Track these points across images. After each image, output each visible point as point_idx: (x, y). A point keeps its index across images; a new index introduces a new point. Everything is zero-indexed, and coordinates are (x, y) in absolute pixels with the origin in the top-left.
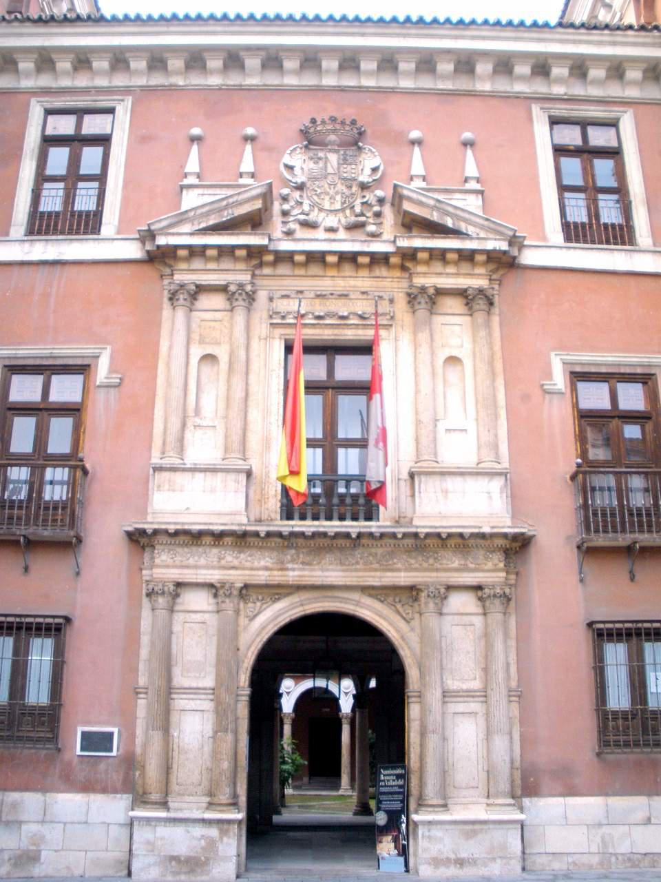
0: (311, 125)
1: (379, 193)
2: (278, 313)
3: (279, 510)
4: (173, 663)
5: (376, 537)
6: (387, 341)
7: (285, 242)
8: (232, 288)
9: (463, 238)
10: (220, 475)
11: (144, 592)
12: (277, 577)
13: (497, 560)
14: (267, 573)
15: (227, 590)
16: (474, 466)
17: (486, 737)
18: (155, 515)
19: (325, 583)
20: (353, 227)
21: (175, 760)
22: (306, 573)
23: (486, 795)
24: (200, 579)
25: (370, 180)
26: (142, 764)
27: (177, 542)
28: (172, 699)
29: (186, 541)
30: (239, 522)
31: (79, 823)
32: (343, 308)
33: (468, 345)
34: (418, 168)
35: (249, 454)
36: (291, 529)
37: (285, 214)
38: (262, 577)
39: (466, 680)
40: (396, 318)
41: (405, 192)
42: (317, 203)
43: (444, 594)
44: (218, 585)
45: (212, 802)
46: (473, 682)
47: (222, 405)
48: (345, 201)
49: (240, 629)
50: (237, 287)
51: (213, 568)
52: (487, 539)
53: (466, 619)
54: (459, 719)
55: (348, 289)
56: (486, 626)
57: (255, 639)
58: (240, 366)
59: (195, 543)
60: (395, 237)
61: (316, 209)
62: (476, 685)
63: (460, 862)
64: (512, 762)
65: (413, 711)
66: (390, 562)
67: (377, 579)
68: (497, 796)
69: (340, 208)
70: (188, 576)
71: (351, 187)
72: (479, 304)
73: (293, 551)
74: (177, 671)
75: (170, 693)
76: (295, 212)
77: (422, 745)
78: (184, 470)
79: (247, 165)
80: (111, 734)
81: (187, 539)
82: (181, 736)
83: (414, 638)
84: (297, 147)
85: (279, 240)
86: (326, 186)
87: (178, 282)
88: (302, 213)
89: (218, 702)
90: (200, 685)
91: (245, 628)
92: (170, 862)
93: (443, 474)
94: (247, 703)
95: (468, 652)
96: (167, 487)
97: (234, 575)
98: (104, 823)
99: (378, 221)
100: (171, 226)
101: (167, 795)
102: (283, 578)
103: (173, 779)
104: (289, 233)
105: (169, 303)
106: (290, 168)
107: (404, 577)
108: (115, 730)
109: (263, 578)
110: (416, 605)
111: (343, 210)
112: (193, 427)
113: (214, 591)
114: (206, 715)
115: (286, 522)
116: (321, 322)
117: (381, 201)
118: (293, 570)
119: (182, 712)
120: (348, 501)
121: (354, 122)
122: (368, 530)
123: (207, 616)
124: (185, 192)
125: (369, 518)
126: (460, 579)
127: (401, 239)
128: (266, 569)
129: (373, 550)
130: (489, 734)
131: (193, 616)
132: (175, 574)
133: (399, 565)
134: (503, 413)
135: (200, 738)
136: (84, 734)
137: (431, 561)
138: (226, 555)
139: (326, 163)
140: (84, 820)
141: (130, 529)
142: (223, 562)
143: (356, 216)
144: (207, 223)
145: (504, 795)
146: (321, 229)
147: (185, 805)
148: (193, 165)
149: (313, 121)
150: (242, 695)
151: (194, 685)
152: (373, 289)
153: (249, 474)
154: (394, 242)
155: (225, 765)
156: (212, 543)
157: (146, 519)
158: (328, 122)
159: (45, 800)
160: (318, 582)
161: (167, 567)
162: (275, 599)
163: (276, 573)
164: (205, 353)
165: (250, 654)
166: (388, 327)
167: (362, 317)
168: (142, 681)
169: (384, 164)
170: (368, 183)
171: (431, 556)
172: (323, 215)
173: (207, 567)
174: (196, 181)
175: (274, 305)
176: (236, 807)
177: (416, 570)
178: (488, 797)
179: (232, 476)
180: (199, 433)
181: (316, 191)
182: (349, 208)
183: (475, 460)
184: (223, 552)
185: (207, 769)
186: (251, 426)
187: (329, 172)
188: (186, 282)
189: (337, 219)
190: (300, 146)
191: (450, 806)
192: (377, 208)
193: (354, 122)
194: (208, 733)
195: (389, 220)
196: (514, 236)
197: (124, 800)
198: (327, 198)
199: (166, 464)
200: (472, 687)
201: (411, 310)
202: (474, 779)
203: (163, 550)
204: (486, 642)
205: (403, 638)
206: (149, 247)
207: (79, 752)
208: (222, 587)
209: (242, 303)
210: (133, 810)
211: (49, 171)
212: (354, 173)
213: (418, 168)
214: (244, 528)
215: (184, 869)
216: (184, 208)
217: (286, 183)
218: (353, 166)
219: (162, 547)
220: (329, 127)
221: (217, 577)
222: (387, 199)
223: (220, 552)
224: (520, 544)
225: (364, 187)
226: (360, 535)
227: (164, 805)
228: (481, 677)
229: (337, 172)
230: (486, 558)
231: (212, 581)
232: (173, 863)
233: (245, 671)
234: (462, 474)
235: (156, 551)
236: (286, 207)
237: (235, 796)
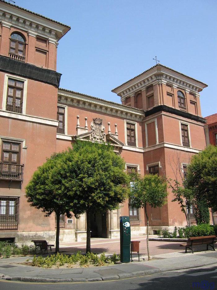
1: (105, 134)
88: (94, 135)
108: (72, 219)
117: (104, 135)
225: (102, 132)
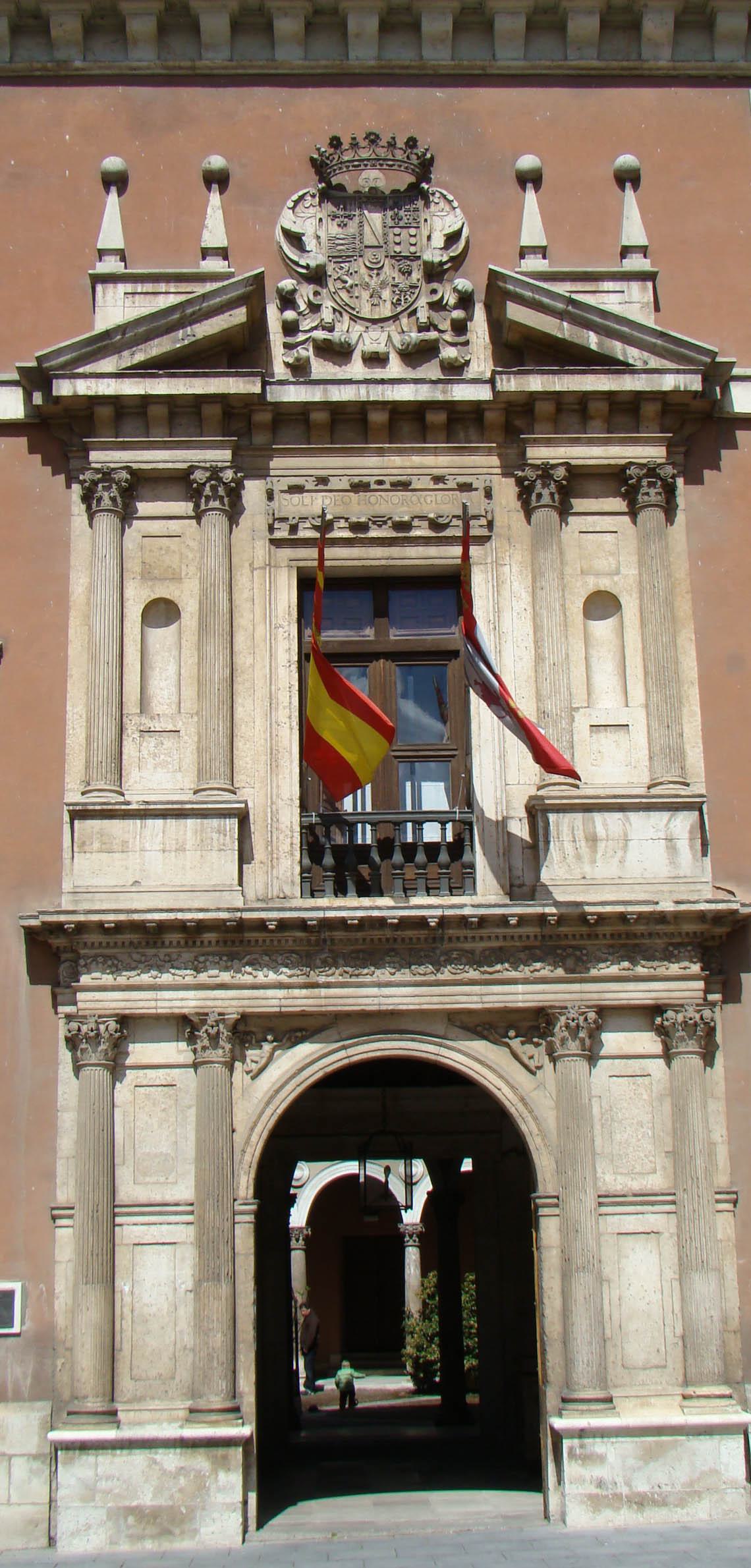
0: (332, 150)
1: (462, 283)
2: (284, 520)
3: (298, 879)
5: (472, 923)
6: (482, 567)
7: (292, 387)
8: (199, 476)
10: (190, 823)
11: (62, 1032)
15: (212, 1027)
16: (642, 791)
17: (677, 1276)
18: (80, 896)
19: (384, 1008)
20: (415, 355)
21: (127, 1334)
23: (681, 1379)
25: (445, 259)
26: (68, 1345)
32: (398, 506)
33: (630, 571)
34: (532, 231)
35: (239, 780)
36: (320, 914)
37: (290, 328)
38: (272, 1001)
39: (640, 1173)
40: (497, 524)
42: (347, 305)
43: (595, 1022)
44: (195, 1019)
45: (195, 1406)
46: (651, 1177)
48: (399, 300)
49: (236, 1095)
50: (208, 474)
52: (669, 923)
53: (635, 1066)
54: (629, 1242)
55: (409, 471)
57: (262, 1112)
58: (222, 624)
60: (494, 373)
61: (346, 317)
62: (656, 1182)
63: (640, 1502)
64: (725, 1320)
65: (549, 1231)
67: (475, 998)
68: (700, 1383)
69: (390, 315)
70: (141, 1004)
71: (410, 273)
72: (647, 494)
74: (124, 1174)
75: (115, 1215)
76: (305, 325)
77: (566, 1295)
79: (215, 234)
81: (135, 937)
82: (136, 1291)
84: (306, 193)
85: (281, 383)
86: (363, 270)
89: (202, 1227)
90: (169, 1198)
92: (126, 1520)
94: (252, 1226)
95: (641, 1124)
99: (462, 339)
101: (113, 1400)
102: (311, 1001)
103: (122, 1368)
104: (299, 369)
105: (83, 507)
106: (295, 239)
108: (17, 1286)
111: (395, 318)
112: (137, 735)
114: (179, 1250)
115: (312, 902)
120: (421, 857)
121: (412, 143)
122: (458, 912)
124: (99, 288)
127: (504, 376)
130: (685, 1268)
131: (151, 1073)
132: (116, 1002)
134: (693, 694)
135: (171, 1297)
138: (208, 963)
139: (361, 225)
141: (34, 923)
143: (421, 329)
145: (714, 1383)
147: (146, 1415)
148: (111, 234)
149: (335, 143)
151: (158, 1198)
153: (243, 818)
154: (492, 382)
155: (219, 1339)
157: (60, 905)
158: (363, 143)
162: (297, 1037)
163: (296, 992)
165: (254, 1138)
166: (483, 540)
167: (435, 525)
168: (65, 1193)
169: (469, 226)
170: (441, 264)
171: (569, 955)
172: (358, 328)
175: (275, 504)
176: (239, 1415)
178: (686, 1383)
180: (150, 743)
181: (346, 282)
182: (405, 314)
183: (646, 780)
184: (202, 959)
185: (185, 1348)
186: (241, 730)
187: (367, 243)
188: (112, 465)
189: (384, 336)
190: (313, 191)
192: (458, 314)
193: (412, 143)
194: (183, 1283)
195: (480, 333)
196: (715, 365)
197: (39, 1411)
198: (365, 295)
199: (94, 804)
200: (649, 1186)
202: (658, 1351)
204: (674, 1105)
205: (522, 1099)
208: (204, 1022)
210: (52, 1428)
212: (415, 245)
213: (532, 231)
214: (239, 915)
215: (151, 1530)
216: (101, 326)
217: (290, 266)
218: (413, 231)
220: (364, 154)
221: (193, 1003)
222: (476, 297)
224: (729, 930)
225: (434, 273)
226: (443, 921)
227: (110, 1416)
228: (664, 1168)
229: (382, 243)
232: (131, 1520)
233: (247, 1167)
234: (622, 808)
236: (290, 315)
237: (234, 1394)
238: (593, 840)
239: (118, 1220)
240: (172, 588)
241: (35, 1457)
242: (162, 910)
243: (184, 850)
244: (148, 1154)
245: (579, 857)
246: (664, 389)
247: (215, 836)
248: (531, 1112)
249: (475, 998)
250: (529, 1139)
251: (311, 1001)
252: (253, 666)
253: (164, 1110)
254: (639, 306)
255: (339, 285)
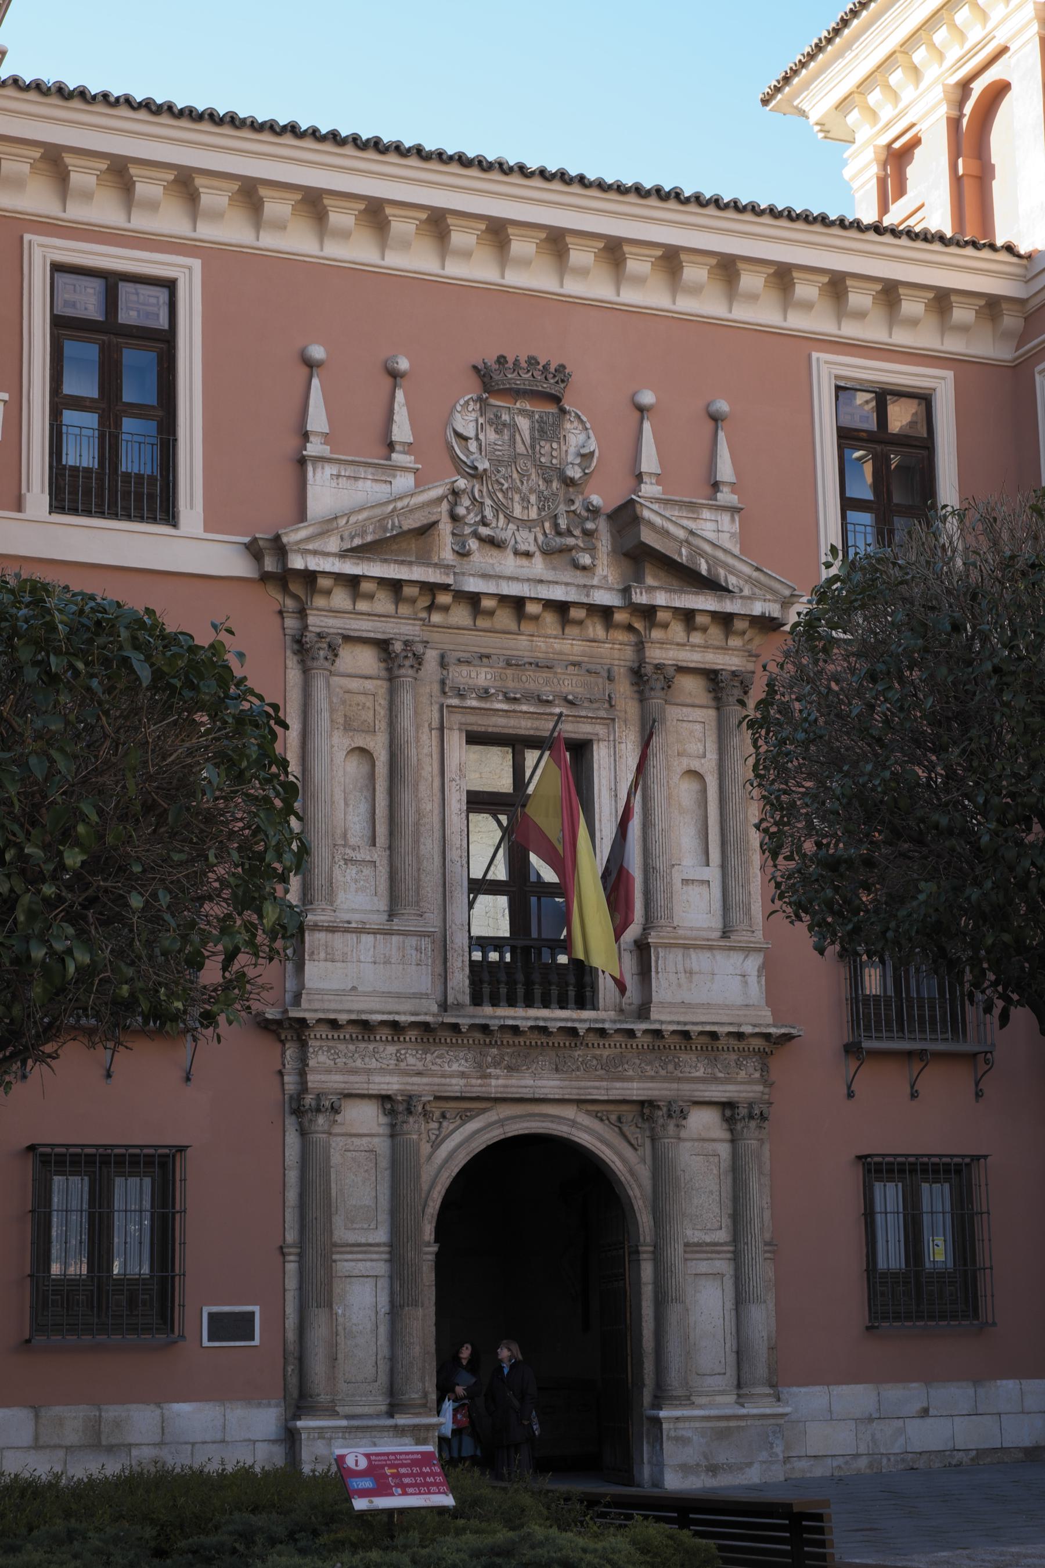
1: (596, 500)
3: (467, 990)
4: (333, 1209)
6: (606, 743)
7: (471, 579)
9: (721, 596)
12: (476, 1086)
13: (751, 1069)
14: (462, 1082)
22: (513, 1082)
23: (735, 1383)
24: (374, 1089)
27: (342, 1037)
28: (335, 1261)
29: (354, 1036)
30: (429, 1012)
31: (214, 1442)
33: (712, 756)
38: (456, 1086)
41: (646, 514)
47: (382, 830)
49: (422, 1161)
51: (391, 1073)
53: (710, 1147)
56: (735, 1155)
59: (366, 1037)
61: (501, 516)
66: (620, 1069)
67: (603, 1092)
70: (357, 1086)
71: (551, 481)
73: (494, 1051)
75: (332, 1253)
76: (472, 518)
78: (347, 930)
80: (253, 1313)
83: (644, 1172)
86: (515, 475)
87: (318, 630)
88: (484, 523)
90: (371, 1241)
91: (430, 1157)
93: (686, 947)
94: (433, 1264)
95: (711, 1192)
96: (322, 955)
97: (418, 1085)
98: (250, 1440)
100: (308, 539)
102: (484, 1089)
105: (295, 658)
106: (462, 438)
107: (638, 1089)
109: (457, 1088)
110: (646, 1126)
111: (541, 522)
112: (342, 863)
113: (388, 1106)
116: (518, 708)
117: (594, 512)
118: (497, 1078)
119: (348, 1280)
122: (600, 1026)
123: (376, 1140)
125: (581, 1003)
126: (707, 1094)
128: (463, 1075)
129: (598, 1052)
130: (740, 1301)
131: (357, 1141)
132: (336, 1081)
133: (631, 1073)
135: (373, 1318)
136: (211, 1315)
137: (671, 1067)
140: (219, 1437)
142: (403, 1065)
143: (559, 533)
144: (362, 537)
146: (509, 552)
148: (317, 420)
150: (426, 1253)
151: (363, 1241)
152: (586, 659)
156: (390, 1038)
158: (524, 365)
159: (162, 1416)
160: (527, 1093)
161: (329, 1071)
163: (474, 1081)
164: (354, 745)
167: (571, 703)
173: (382, 1071)
174: (325, 450)
177: (652, 1079)
179: (413, 941)
180: (352, 871)
181: (503, 485)
184: (403, 1052)
191: (693, 1398)
198: (517, 497)
199: (323, 921)
201: (636, 696)
203: (321, 1047)
206: (270, 565)
207: (206, 1343)
209: (410, 672)
211: (70, 388)
219: (318, 1043)
221: (396, 1087)
223: (398, 1051)
225: (569, 482)
230: (739, 1065)
231: (390, 1092)
235: (311, 1050)
237: (425, 1395)
238: (690, 973)
239: (335, 1257)
240: (368, 739)
241: (274, 1442)
242: (383, 1013)
243: (390, 963)
244: (355, 1206)
245: (679, 986)
246: (754, 613)
247: (414, 952)
248: (636, 1180)
249: (603, 1092)
250: (634, 1201)
251: (484, 1089)
252: (432, 811)
253: (366, 1171)
254: (728, 535)
255: (496, 486)
